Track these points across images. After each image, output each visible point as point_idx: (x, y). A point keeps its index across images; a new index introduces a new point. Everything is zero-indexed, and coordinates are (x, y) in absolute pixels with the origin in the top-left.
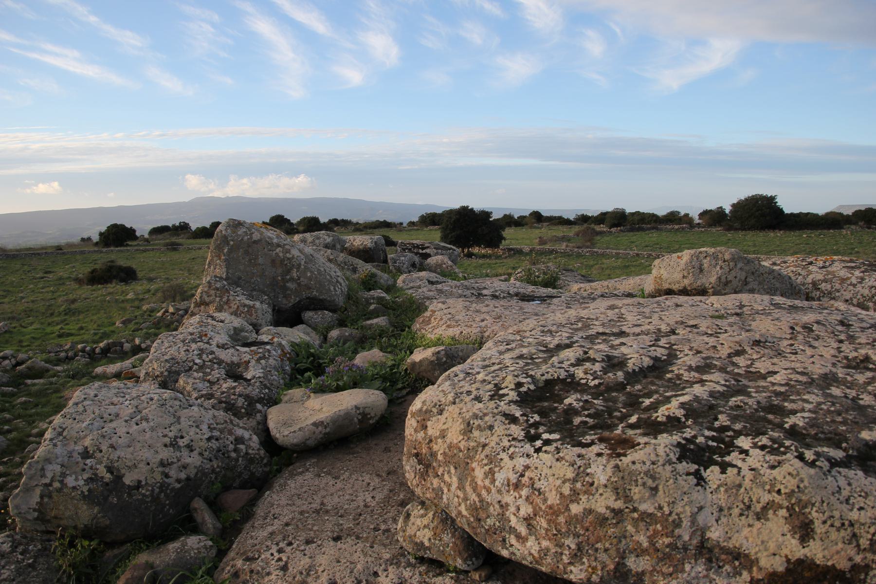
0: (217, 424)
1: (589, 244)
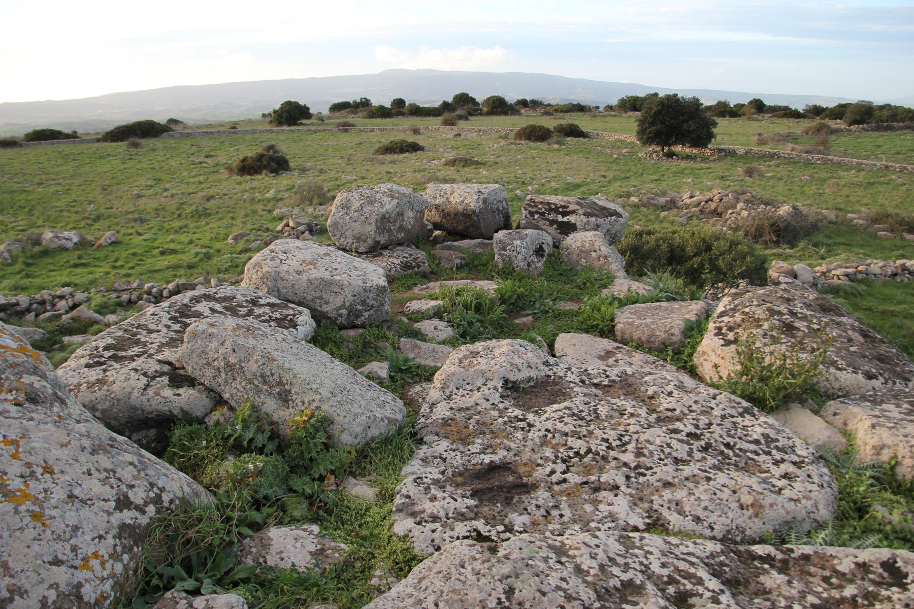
1: (822, 148)
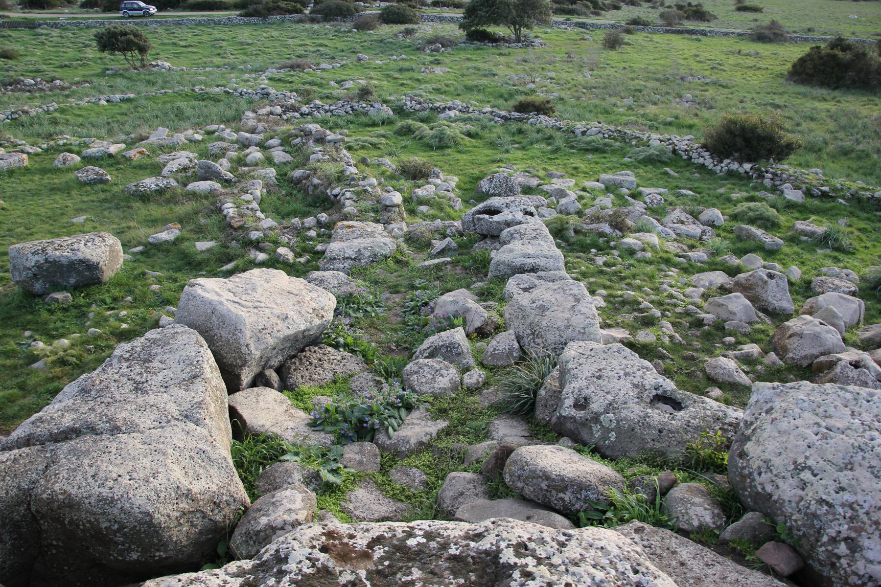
0: (867, 513)
